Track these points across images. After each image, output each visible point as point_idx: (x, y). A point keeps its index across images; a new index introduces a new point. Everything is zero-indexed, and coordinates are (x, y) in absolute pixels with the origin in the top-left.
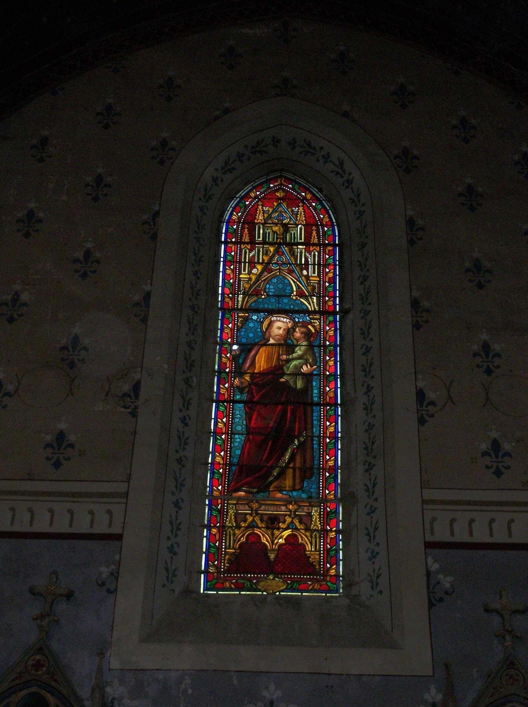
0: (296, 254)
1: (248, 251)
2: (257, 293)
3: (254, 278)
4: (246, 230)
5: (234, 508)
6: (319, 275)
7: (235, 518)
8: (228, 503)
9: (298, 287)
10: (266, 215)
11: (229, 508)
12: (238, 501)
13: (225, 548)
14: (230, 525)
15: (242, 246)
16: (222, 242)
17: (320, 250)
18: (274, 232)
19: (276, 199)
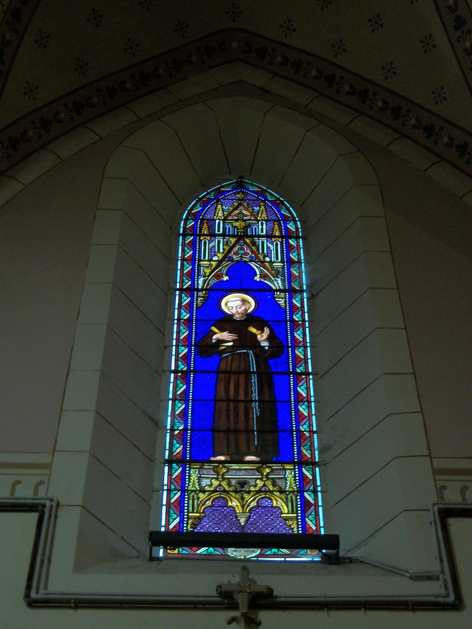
0: (257, 244)
1: (207, 241)
2: (218, 276)
3: (214, 264)
4: (205, 225)
5: (197, 472)
6: (282, 262)
7: (198, 482)
8: (190, 468)
9: (261, 271)
10: (226, 213)
11: (191, 473)
12: (201, 466)
13: (188, 512)
14: (194, 489)
15: (202, 238)
16: (180, 235)
17: (282, 240)
18: (235, 227)
19: (236, 200)
